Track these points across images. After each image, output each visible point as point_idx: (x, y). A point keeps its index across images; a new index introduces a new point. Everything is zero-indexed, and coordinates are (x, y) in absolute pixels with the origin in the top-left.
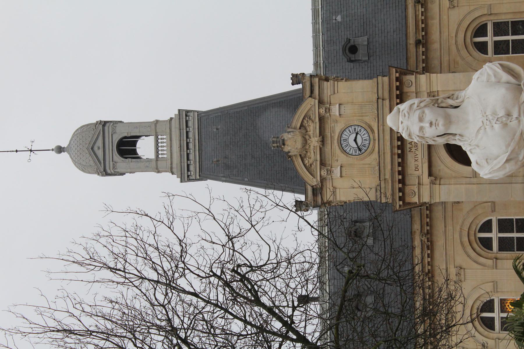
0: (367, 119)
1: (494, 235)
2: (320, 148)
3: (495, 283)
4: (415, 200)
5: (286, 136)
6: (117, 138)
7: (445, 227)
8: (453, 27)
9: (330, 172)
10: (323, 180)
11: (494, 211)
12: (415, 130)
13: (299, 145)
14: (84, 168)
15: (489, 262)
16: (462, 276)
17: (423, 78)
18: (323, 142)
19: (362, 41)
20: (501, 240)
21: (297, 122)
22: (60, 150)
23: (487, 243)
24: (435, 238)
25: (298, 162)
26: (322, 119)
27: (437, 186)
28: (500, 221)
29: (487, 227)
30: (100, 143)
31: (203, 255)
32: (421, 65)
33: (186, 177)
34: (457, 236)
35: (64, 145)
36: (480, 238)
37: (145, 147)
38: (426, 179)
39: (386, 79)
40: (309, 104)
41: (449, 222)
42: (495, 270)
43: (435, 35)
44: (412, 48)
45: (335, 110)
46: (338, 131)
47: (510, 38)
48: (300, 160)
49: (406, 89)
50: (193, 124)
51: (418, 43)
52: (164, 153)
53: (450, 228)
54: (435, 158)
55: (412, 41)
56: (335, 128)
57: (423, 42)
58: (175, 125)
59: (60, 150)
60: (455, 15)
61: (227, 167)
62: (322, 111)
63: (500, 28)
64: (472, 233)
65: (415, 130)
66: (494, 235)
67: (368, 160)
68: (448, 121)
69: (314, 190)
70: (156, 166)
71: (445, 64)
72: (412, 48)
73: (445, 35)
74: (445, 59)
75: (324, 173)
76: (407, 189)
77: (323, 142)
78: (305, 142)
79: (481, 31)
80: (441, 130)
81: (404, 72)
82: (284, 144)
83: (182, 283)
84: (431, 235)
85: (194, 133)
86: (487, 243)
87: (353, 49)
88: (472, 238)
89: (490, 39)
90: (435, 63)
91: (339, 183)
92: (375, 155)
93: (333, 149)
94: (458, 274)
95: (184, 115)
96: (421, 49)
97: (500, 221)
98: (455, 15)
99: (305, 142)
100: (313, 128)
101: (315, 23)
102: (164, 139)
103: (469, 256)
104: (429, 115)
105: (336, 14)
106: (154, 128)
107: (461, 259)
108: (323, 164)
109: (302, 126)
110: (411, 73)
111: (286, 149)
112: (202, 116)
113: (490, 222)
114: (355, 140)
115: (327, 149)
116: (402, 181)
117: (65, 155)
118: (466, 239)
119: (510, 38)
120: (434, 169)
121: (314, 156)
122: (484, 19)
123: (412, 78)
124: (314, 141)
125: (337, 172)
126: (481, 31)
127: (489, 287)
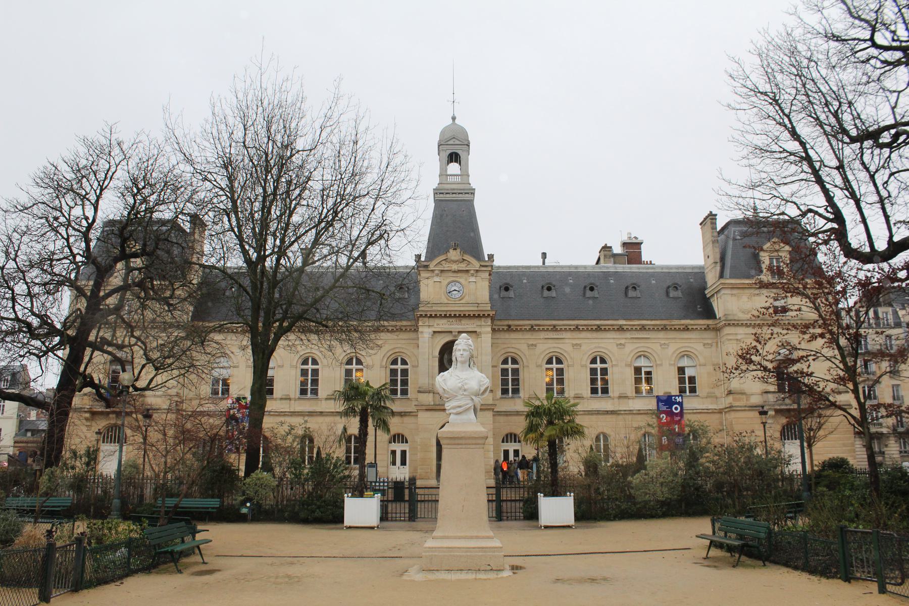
0: (467, 297)
1: (399, 367)
4: (420, 323)
5: (458, 250)
6: (459, 152)
8: (517, 346)
9: (437, 275)
10: (433, 271)
11: (413, 366)
12: (459, 347)
13: (453, 258)
14: (443, 133)
15: (384, 363)
17: (489, 329)
18: (454, 272)
19: (511, 294)
21: (467, 257)
22: (454, 118)
23: (395, 362)
25: (443, 257)
26: (467, 271)
28: (407, 370)
29: (404, 362)
30: (457, 142)
31: (395, 217)
32: (497, 328)
33: (437, 192)
34: (399, 345)
35: (456, 121)
37: (454, 168)
39: (489, 308)
40: (476, 264)
43: (513, 335)
44: (506, 323)
45: (472, 279)
47: (510, 377)
49: (483, 319)
50: (467, 197)
51: (509, 326)
52: (450, 179)
53: (404, 342)
54: (443, 335)
55: (511, 323)
56: (462, 278)
57: (509, 329)
58: (467, 186)
59: (454, 118)
60: (524, 347)
61: (442, 216)
62: (472, 272)
63: (516, 372)
65: (459, 347)
66: (399, 367)
67: (443, 297)
68: (463, 363)
69: (427, 266)
70: (443, 174)
71: (496, 341)
72: (506, 323)
73: (513, 341)
74: (499, 341)
75: (437, 272)
76: (426, 319)
78: (455, 262)
79: (515, 361)
80: (459, 359)
81: (493, 319)
83: (379, 203)
85: (461, 197)
86: (395, 362)
87: (507, 289)
89: (510, 366)
90: (498, 335)
91: (430, 282)
92: (446, 301)
93: (450, 277)
95: (472, 192)
96: (506, 328)
97: (407, 370)
98: (524, 347)
99: (455, 262)
100: (463, 266)
101: (523, 267)
102: (459, 179)
104: (466, 354)
105: (528, 279)
106: (465, 174)
108: (442, 271)
110: (492, 322)
111: (451, 251)
112: (471, 203)
115: (450, 274)
116: (431, 316)
117: (451, 121)
119: (510, 377)
120: (437, 334)
121: (446, 266)
122: (521, 363)
123: (489, 323)
124: (455, 267)
125: (437, 279)
126: (515, 361)
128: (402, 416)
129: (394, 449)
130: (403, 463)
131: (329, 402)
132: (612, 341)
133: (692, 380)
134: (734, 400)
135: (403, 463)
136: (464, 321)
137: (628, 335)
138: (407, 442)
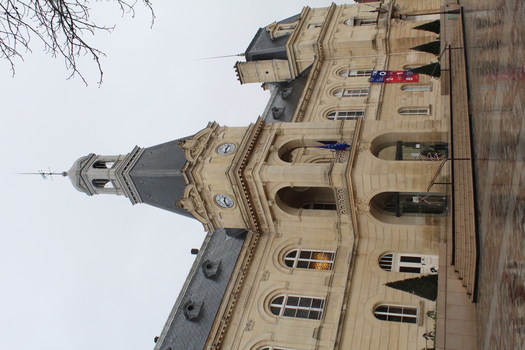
2: (204, 150)
3: (288, 283)
7: (265, 248)
10: (198, 162)
11: (300, 243)
16: (267, 277)
18: (207, 147)
20: (299, 262)
22: (65, 174)
24: (256, 255)
27: (267, 166)
29: (293, 254)
30: (86, 162)
34: (271, 254)
36: (286, 261)
38: (262, 162)
41: (269, 246)
42: (290, 275)
46: (218, 144)
48: (189, 152)
53: (268, 250)
59: (65, 174)
64: (282, 255)
77: (207, 147)
82: (184, 143)
84: (255, 252)
88: (281, 257)
94: (264, 275)
103: (275, 266)
107: (269, 267)
109: (199, 139)
113: (295, 252)
114: (226, 149)
118: (276, 257)
121: (199, 151)
127: (283, 285)
128: (357, 255)
129: (398, 269)
130: (418, 260)
131: (322, 336)
132: (316, 107)
133: (359, 73)
134: (380, 37)
135: (418, 260)
136: (262, 141)
137: (313, 99)
138: (391, 255)
